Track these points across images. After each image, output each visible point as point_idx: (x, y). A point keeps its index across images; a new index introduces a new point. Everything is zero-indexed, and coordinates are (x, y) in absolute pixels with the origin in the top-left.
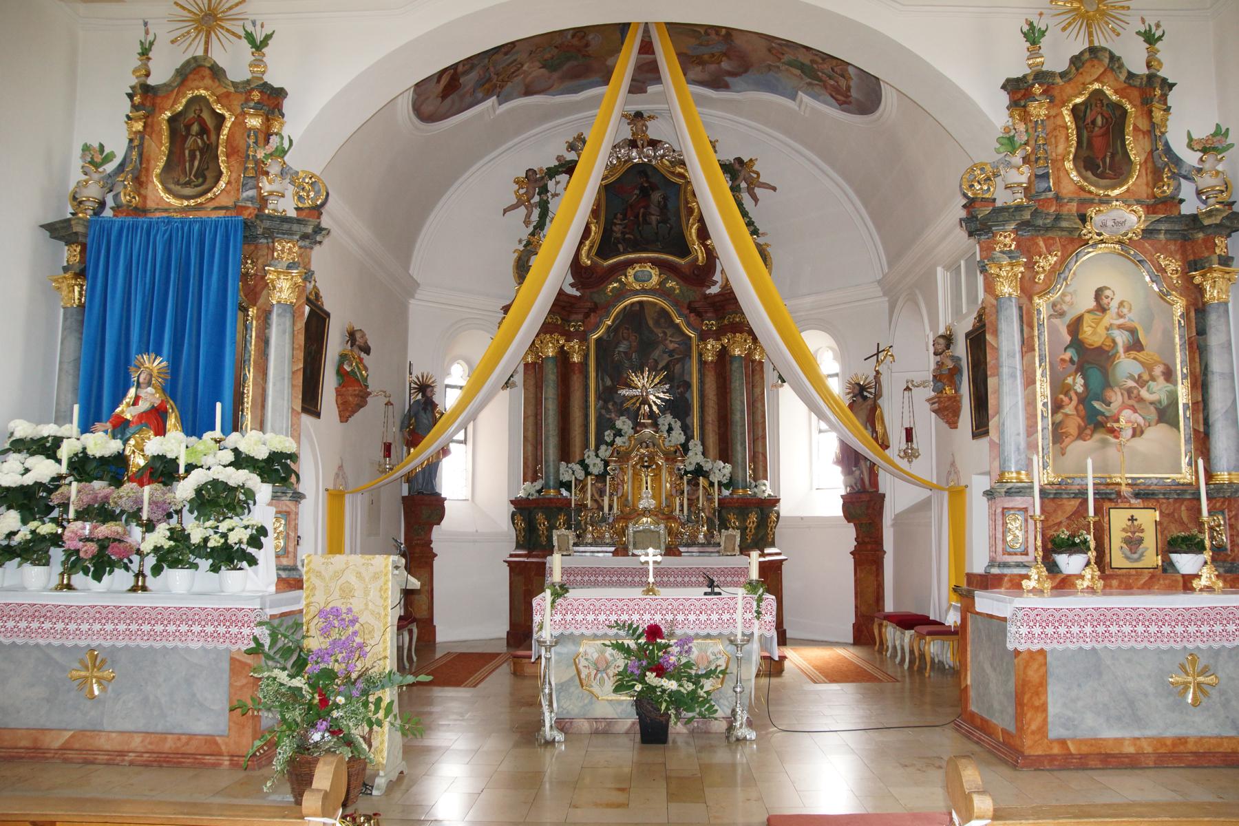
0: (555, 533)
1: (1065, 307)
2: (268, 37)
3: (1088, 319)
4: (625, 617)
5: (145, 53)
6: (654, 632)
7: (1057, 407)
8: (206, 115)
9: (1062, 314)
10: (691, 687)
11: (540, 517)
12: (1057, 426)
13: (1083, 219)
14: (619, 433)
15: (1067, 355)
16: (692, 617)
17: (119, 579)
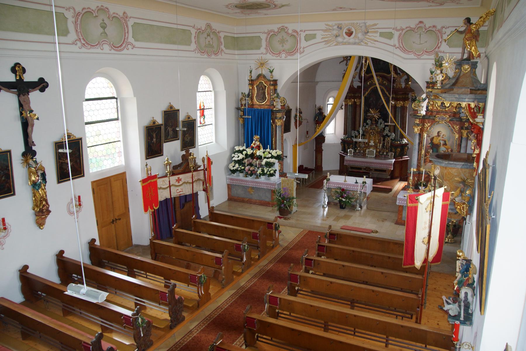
0: (348, 150)
1: (430, 135)
2: (273, 70)
3: (435, 138)
4: (339, 186)
5: (251, 72)
6: (343, 190)
7: (426, 155)
8: (263, 86)
9: (429, 136)
10: (348, 200)
11: (346, 145)
12: (425, 160)
13: (435, 117)
14: (367, 124)
15: (429, 145)
16: (351, 187)
17: (254, 176)
